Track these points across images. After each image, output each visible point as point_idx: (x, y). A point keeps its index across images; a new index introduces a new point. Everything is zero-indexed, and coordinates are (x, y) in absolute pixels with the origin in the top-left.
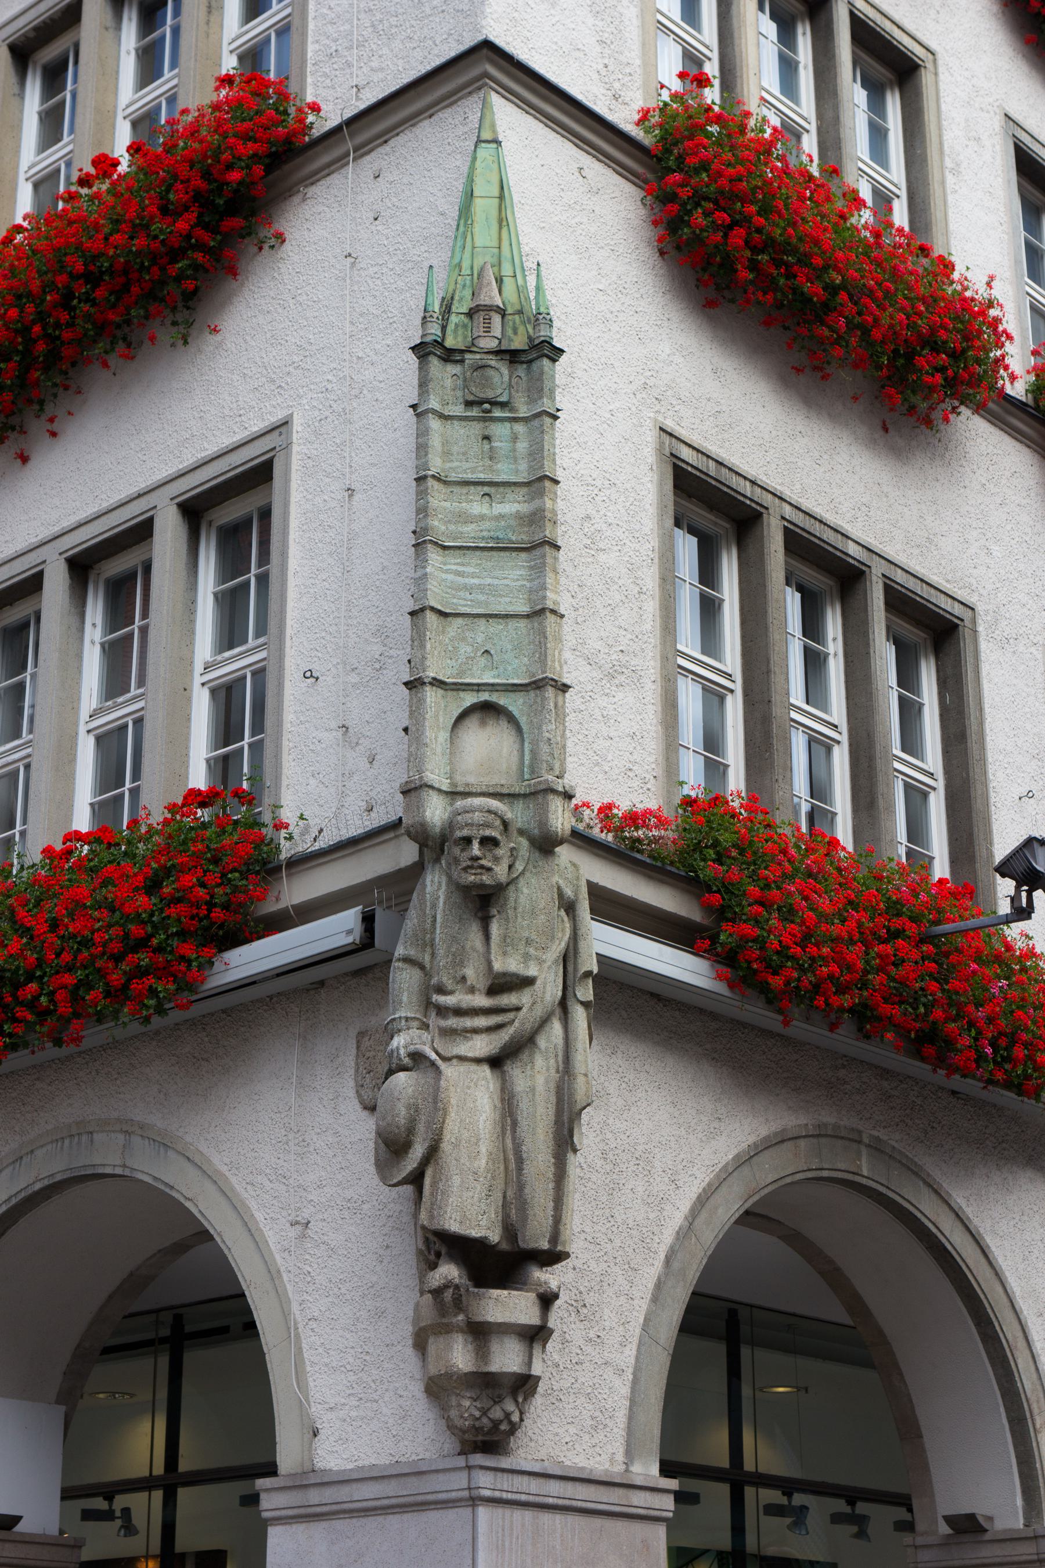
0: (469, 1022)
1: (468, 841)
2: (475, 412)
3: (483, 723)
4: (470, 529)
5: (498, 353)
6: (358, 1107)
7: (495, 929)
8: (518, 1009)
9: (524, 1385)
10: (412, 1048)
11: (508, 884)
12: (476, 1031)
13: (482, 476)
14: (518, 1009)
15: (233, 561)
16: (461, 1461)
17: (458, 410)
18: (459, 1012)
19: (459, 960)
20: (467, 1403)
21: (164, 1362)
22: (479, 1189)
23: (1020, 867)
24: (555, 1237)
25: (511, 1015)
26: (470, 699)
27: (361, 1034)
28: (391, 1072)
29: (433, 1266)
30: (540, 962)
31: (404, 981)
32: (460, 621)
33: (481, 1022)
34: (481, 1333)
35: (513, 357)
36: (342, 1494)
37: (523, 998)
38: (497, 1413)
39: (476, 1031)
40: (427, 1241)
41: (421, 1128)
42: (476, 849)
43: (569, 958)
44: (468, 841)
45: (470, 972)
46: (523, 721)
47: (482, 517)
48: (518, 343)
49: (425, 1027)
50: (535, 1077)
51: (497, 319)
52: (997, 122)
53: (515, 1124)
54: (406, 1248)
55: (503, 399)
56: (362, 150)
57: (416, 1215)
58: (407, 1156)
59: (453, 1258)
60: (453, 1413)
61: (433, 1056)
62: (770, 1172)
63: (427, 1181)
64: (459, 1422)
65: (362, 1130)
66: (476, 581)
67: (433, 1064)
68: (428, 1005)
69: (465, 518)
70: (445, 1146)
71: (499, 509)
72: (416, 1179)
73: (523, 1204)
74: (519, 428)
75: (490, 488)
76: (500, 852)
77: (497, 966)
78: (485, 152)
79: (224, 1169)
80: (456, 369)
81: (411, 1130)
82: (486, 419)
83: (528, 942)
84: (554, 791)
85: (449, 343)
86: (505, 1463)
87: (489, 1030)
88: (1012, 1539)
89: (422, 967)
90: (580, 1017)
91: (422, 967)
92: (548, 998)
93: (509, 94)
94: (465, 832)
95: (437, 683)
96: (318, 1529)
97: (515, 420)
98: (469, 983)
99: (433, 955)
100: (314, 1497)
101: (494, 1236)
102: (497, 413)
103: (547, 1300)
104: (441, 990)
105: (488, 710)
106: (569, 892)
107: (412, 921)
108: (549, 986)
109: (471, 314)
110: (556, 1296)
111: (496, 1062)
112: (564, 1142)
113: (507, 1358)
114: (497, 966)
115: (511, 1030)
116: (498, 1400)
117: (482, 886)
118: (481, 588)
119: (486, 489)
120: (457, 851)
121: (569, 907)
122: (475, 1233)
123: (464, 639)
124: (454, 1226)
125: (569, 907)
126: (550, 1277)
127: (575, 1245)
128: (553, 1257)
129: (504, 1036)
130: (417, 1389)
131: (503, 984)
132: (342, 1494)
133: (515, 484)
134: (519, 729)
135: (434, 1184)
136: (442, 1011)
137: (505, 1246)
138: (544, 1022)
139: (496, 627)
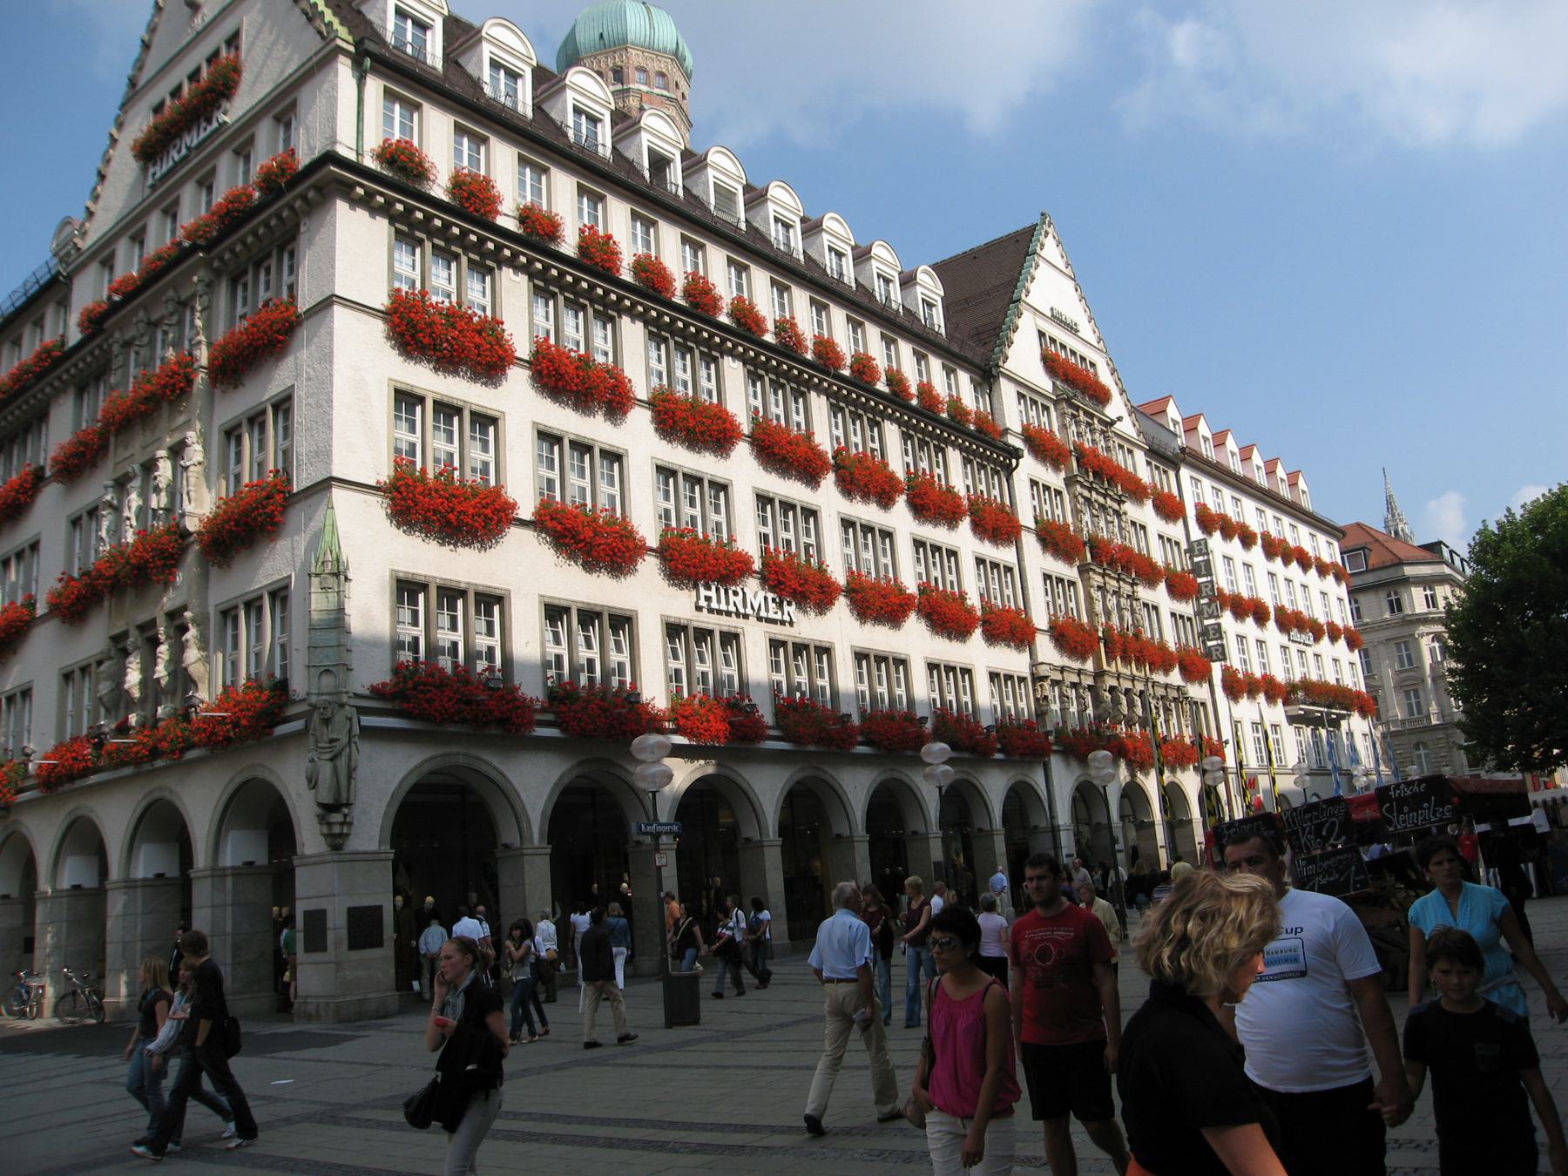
15: (284, 609)
34: (330, 824)
50: (342, 763)
56: (306, 498)
62: (426, 769)
105: (328, 671)
108: (345, 740)
111: (331, 760)
112: (350, 777)
113: (337, 830)
128: (348, 805)
131: (332, 741)
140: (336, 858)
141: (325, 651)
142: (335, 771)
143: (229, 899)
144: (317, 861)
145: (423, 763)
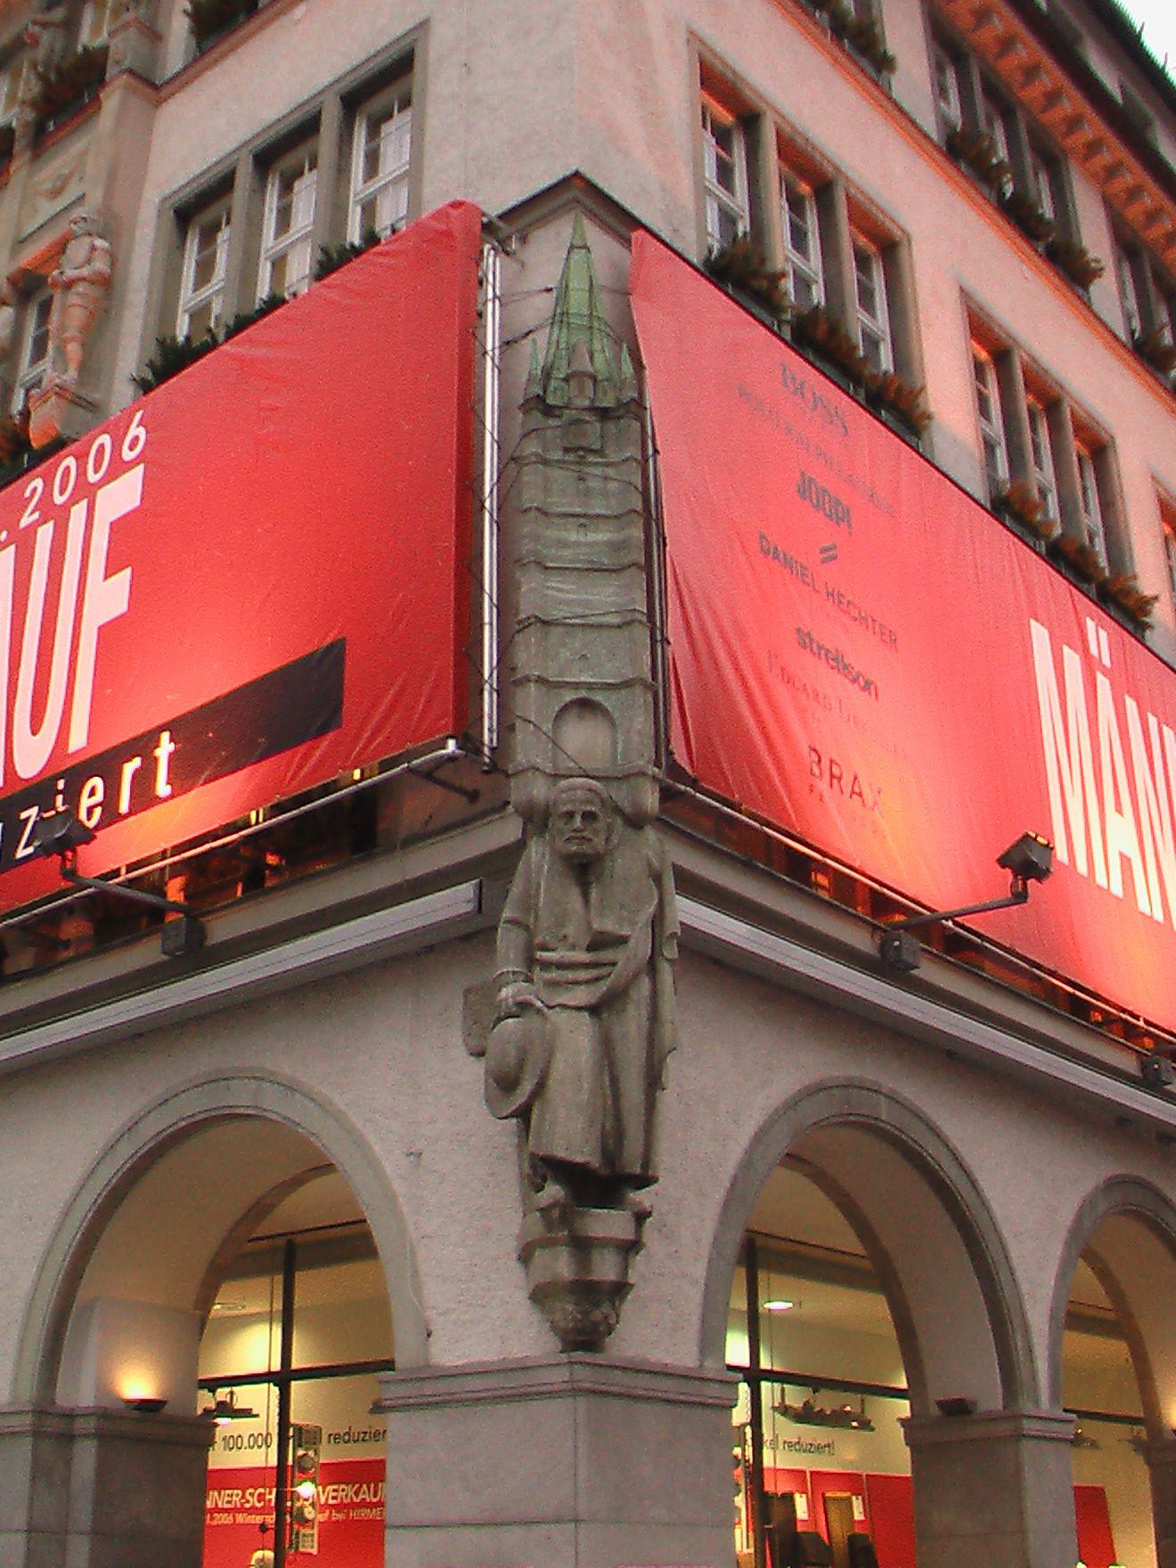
0: (570, 975)
1: (571, 815)
2: (571, 457)
3: (580, 717)
4: (566, 553)
5: (593, 409)
6: (465, 1054)
7: (594, 895)
8: (614, 964)
9: (620, 1289)
10: (520, 998)
11: (606, 853)
12: (576, 983)
13: (578, 510)
14: (614, 964)
16: (564, 1357)
17: (557, 455)
18: (561, 966)
19: (561, 920)
20: (570, 1307)
21: (279, 1278)
22: (579, 1123)
23: (1017, 858)
24: (647, 1162)
25: (608, 969)
26: (569, 696)
27: (467, 992)
28: (500, 1019)
29: (540, 1189)
30: (633, 923)
31: (508, 942)
32: (560, 630)
33: (583, 975)
34: (582, 1246)
35: (604, 414)
36: (455, 1385)
37: (618, 955)
38: (597, 1315)
39: (576, 983)
40: (533, 1167)
41: (529, 1067)
42: (578, 822)
43: (657, 921)
44: (571, 815)
45: (570, 930)
46: (616, 715)
47: (577, 544)
48: (608, 402)
49: (529, 980)
50: (632, 1023)
51: (589, 383)
52: (955, 294)
53: (612, 1065)
54: (509, 1175)
55: (597, 446)
57: (521, 1146)
58: (516, 1091)
59: (557, 1180)
60: (558, 1316)
61: (539, 1004)
62: (812, 1112)
63: (534, 1117)
64: (562, 1324)
65: (474, 1073)
66: (572, 596)
67: (539, 1011)
68: (531, 961)
69: (564, 544)
70: (551, 1082)
71: (592, 537)
72: (524, 1114)
73: (619, 1132)
74: (611, 472)
75: (585, 520)
76: (600, 825)
77: (595, 926)
78: (578, 255)
79: (343, 1107)
80: (556, 422)
81: (521, 1065)
82: (581, 462)
83: (622, 907)
84: (644, 774)
85: (550, 400)
86: (599, 1358)
87: (587, 982)
88: (992, 1418)
89: (527, 928)
90: (666, 974)
91: (527, 928)
92: (640, 954)
93: (592, 216)
94: (569, 807)
95: (541, 680)
96: (430, 1415)
97: (607, 465)
98: (571, 940)
99: (537, 918)
100: (429, 1388)
101: (595, 1162)
102: (591, 458)
103: (641, 1217)
104: (544, 948)
105: (585, 705)
106: (655, 862)
107: (516, 889)
108: (640, 945)
109: (566, 380)
110: (650, 1214)
111: (594, 1010)
112: (654, 1081)
113: (605, 1268)
114: (595, 926)
115: (608, 982)
116: (597, 1305)
117: (584, 855)
118: (579, 603)
119: (582, 520)
120: (561, 824)
121: (657, 879)
122: (579, 1159)
123: (564, 645)
124: (561, 1153)
125: (657, 879)
126: (643, 1197)
127: (662, 1173)
128: (644, 1180)
129: (603, 987)
130: (520, 1297)
131: (600, 942)
132: (455, 1385)
133: (606, 517)
134: (612, 724)
135: (542, 1118)
136: (546, 965)
137: (604, 1172)
138: (636, 976)
139: (591, 635)
140: (585, 1377)
141: (577, 642)
142: (607, 1048)
143: (83, 1513)
144: (503, 1387)
145: (793, 1104)
